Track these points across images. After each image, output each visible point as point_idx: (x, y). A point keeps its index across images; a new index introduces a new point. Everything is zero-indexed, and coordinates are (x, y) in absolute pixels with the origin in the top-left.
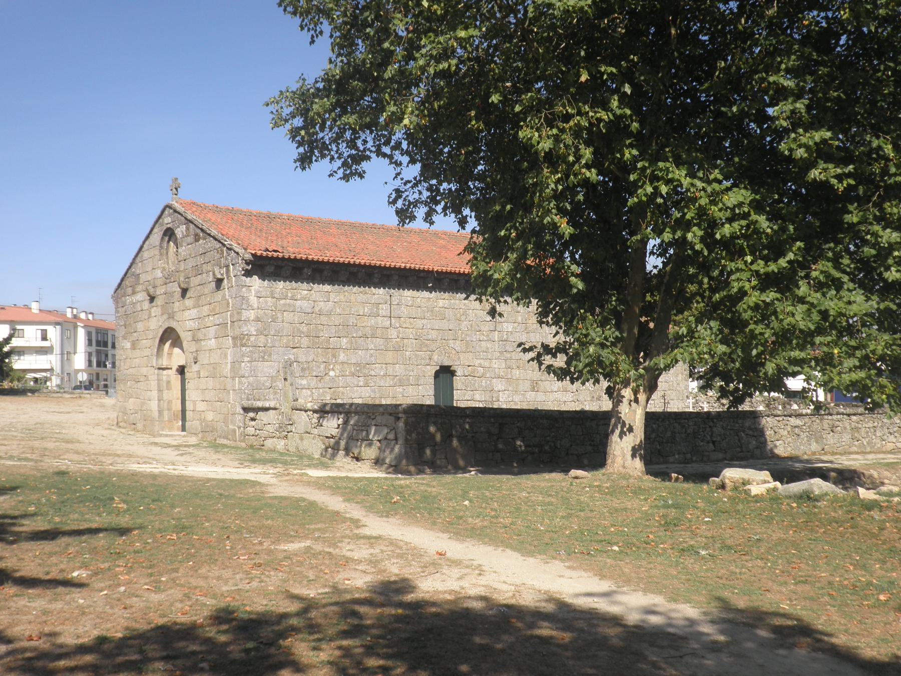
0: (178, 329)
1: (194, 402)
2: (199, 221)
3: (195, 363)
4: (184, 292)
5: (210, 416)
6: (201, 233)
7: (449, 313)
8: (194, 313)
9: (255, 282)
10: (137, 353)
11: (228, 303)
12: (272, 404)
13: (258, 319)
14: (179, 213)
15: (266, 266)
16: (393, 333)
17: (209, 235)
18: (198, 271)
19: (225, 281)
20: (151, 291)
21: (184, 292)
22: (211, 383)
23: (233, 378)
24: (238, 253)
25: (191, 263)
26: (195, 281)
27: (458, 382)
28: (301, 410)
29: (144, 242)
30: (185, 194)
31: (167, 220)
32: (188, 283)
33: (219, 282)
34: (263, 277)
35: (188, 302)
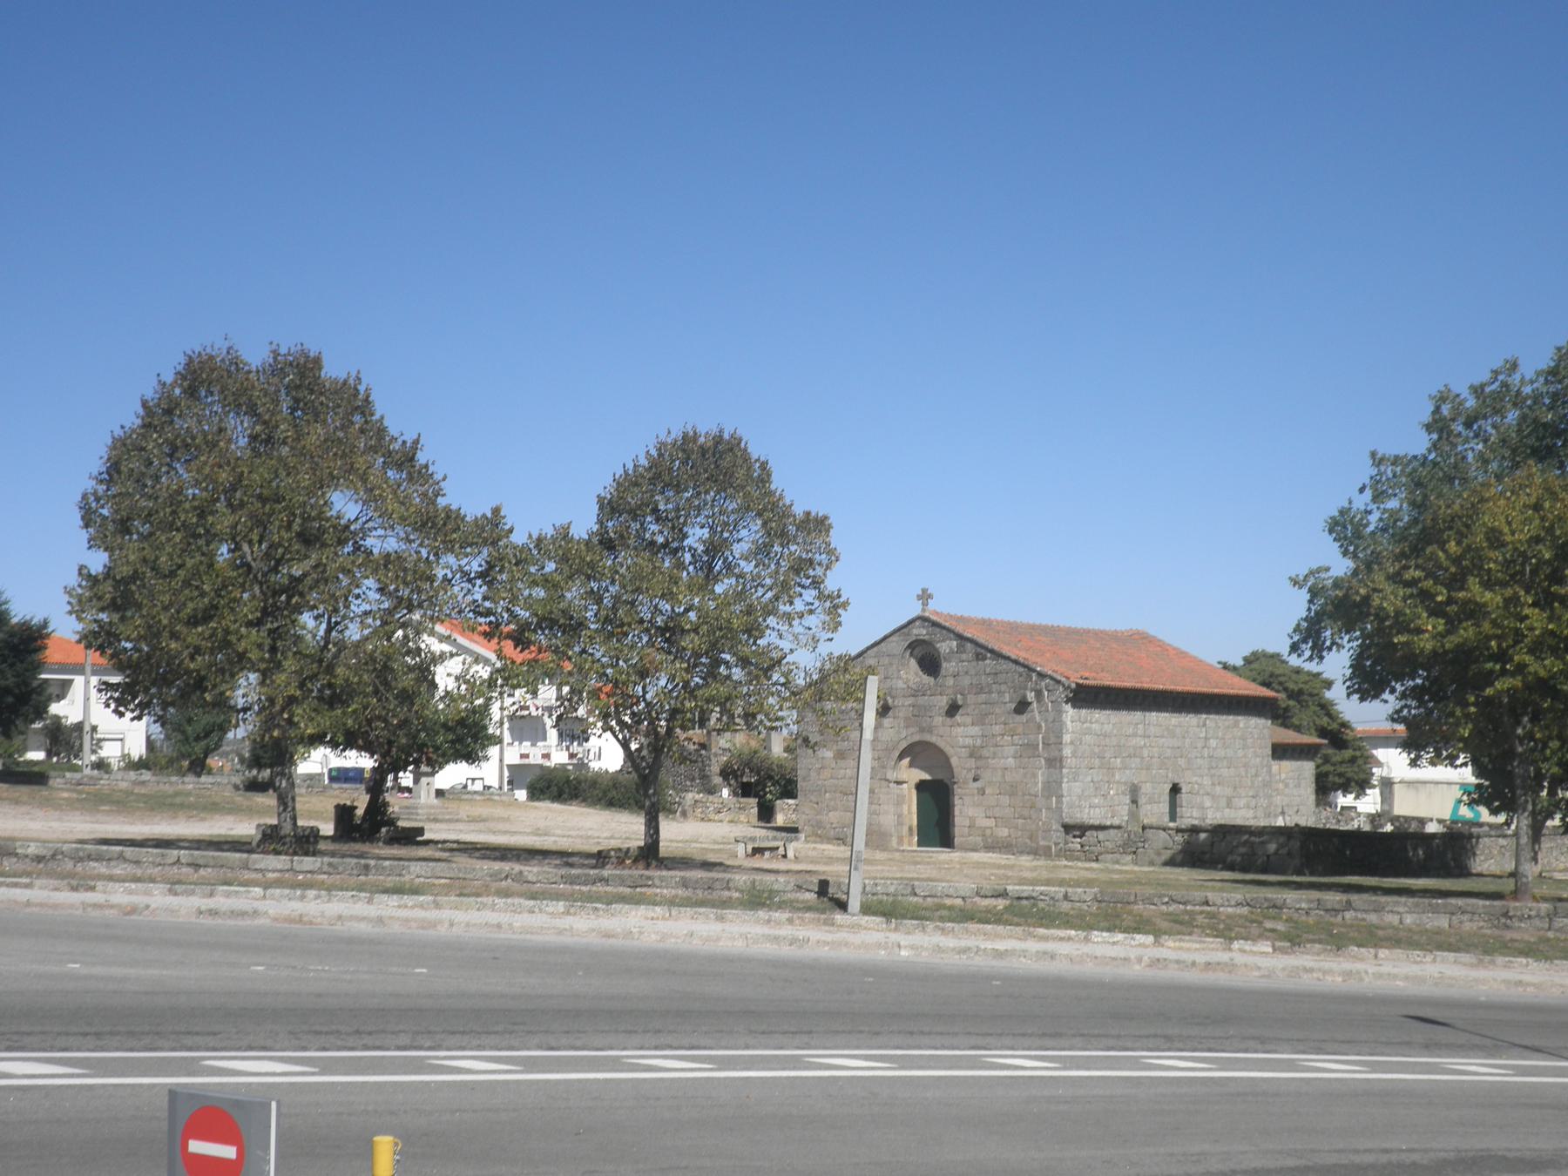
0: (941, 744)
1: (972, 819)
2: (981, 640)
3: (975, 780)
4: (953, 710)
5: (1003, 832)
6: (983, 652)
7: (1178, 730)
8: (976, 730)
9: (1068, 707)
10: (842, 763)
11: (1040, 727)
12: (1116, 822)
13: (1072, 743)
14: (944, 628)
15: (1089, 696)
16: (1145, 753)
17: (1008, 658)
18: (980, 690)
19: (1035, 705)
20: (890, 701)
21: (953, 710)
22: (1005, 800)
23: (1049, 797)
24: (1059, 682)
25: (966, 681)
26: (971, 699)
27: (1183, 798)
28: (1158, 828)
29: (868, 648)
30: (933, 605)
31: (920, 632)
32: (965, 699)
33: (1022, 707)
34: (1074, 707)
35: (958, 718)
